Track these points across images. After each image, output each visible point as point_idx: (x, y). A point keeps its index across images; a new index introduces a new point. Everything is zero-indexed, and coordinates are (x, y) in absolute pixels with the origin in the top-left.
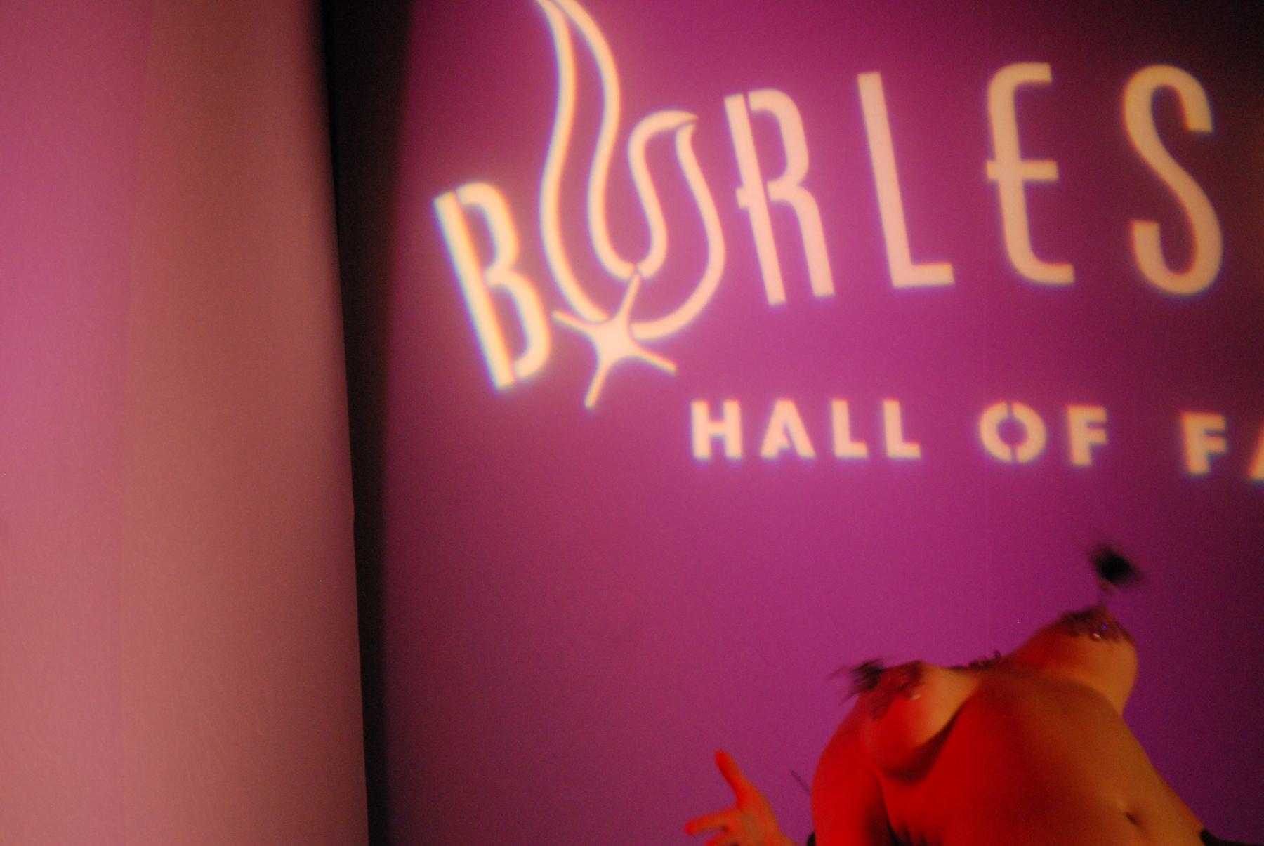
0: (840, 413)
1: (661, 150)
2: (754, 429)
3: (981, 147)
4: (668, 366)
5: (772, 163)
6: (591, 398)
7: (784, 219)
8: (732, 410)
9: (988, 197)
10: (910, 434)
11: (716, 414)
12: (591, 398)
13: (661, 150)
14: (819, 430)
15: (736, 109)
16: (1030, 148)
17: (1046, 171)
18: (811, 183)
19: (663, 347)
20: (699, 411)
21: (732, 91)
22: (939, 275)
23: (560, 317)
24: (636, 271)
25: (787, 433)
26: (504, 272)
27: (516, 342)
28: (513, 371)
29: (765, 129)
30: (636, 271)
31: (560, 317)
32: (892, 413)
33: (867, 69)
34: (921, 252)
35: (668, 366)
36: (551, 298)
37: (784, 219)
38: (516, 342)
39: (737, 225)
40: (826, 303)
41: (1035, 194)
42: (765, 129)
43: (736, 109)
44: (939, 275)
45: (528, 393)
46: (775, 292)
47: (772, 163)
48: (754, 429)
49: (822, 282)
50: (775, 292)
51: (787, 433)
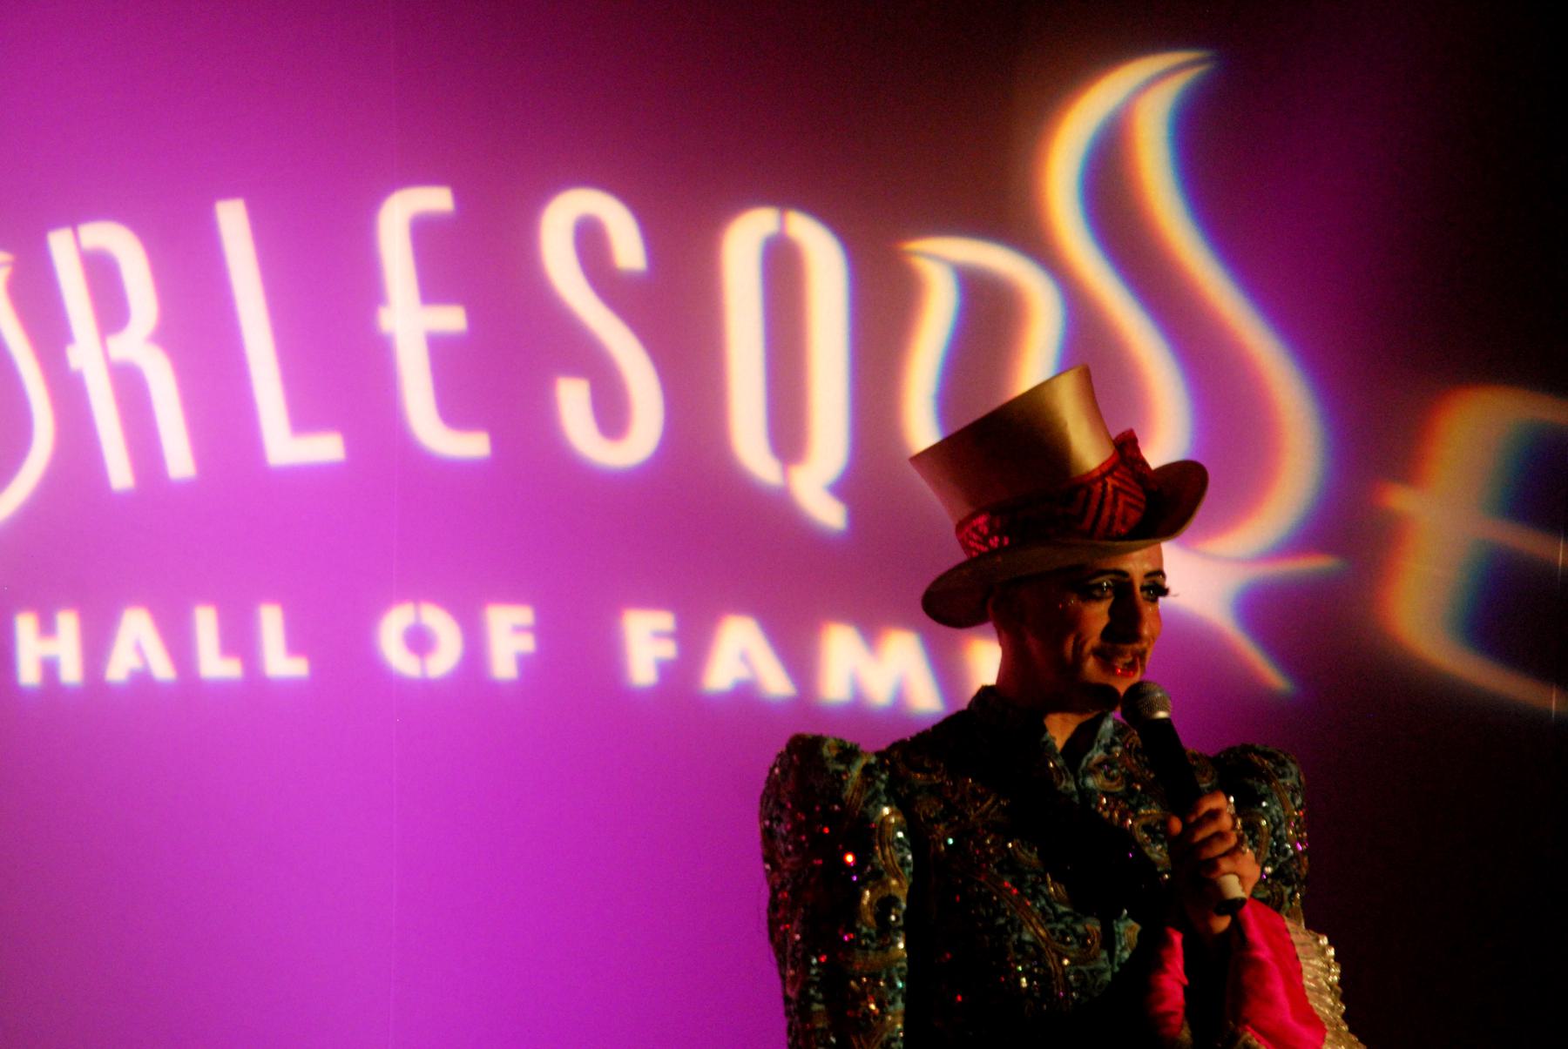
0: (206, 623)
2: (96, 646)
7: (129, 385)
8: (68, 623)
10: (296, 644)
11: (47, 628)
14: (180, 644)
15: (63, 247)
16: (433, 290)
17: (452, 319)
18: (164, 337)
20: (25, 626)
21: (57, 224)
22: (326, 448)
25: (139, 649)
29: (101, 271)
32: (271, 621)
34: (304, 420)
37: (129, 385)
40: (185, 487)
41: (439, 347)
42: (101, 271)
43: (63, 247)
44: (326, 448)
48: (96, 646)
49: (180, 461)
50: (120, 473)
51: (139, 649)
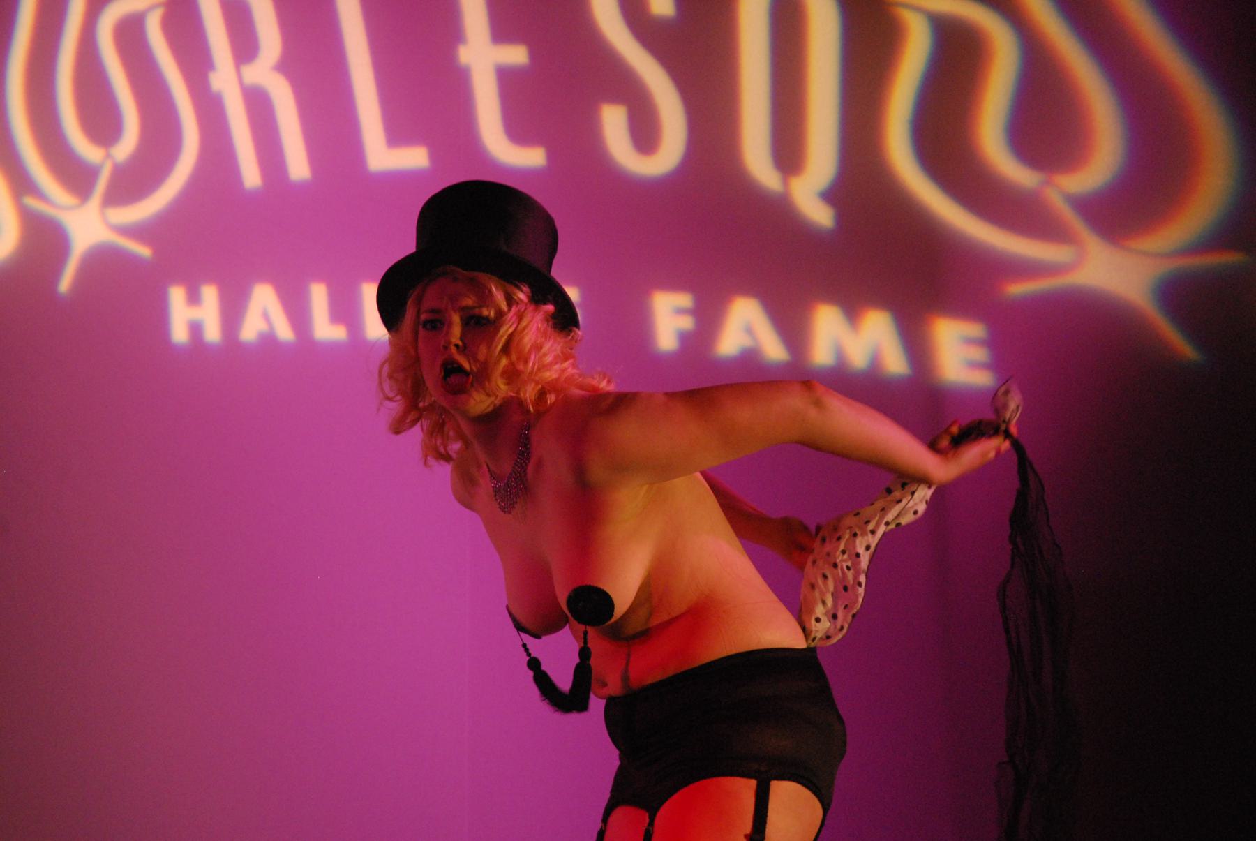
0: (319, 295)
2: (232, 313)
3: (452, 32)
4: (144, 251)
5: (245, 47)
6: (65, 284)
7: (258, 103)
8: (210, 294)
11: (194, 298)
12: (65, 284)
14: (298, 313)
16: (501, 33)
17: (516, 55)
18: (285, 66)
19: (137, 232)
20: (177, 296)
22: (415, 158)
23: (30, 202)
24: (108, 156)
25: (266, 317)
30: (108, 156)
31: (30, 202)
34: (397, 136)
35: (144, 251)
37: (258, 103)
40: (303, 187)
41: (506, 77)
44: (415, 158)
46: (251, 176)
47: (245, 47)
48: (232, 313)
49: (298, 166)
50: (251, 176)
51: (266, 317)
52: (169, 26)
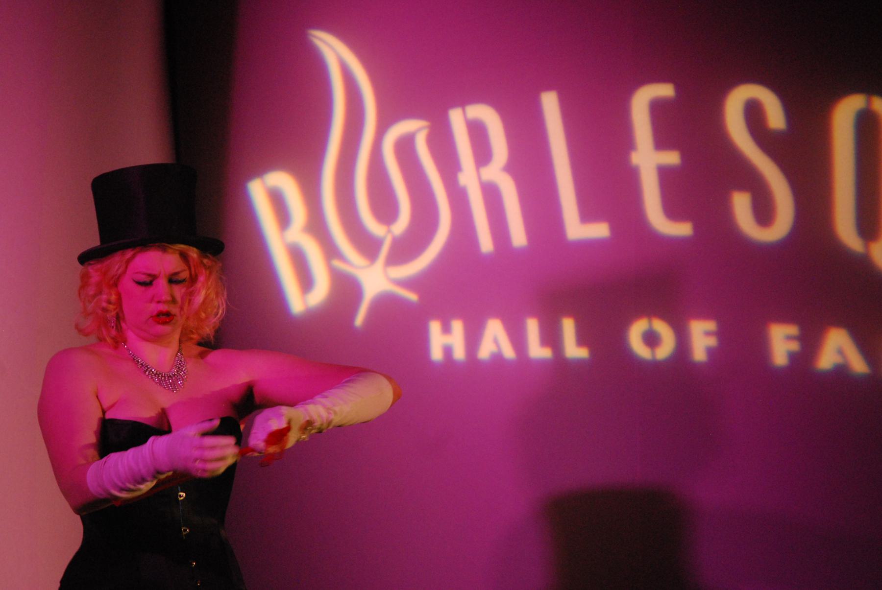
0: (532, 327)
1: (405, 147)
2: (473, 339)
3: (627, 142)
4: (412, 297)
5: (483, 155)
6: (359, 320)
7: (491, 194)
8: (457, 326)
9: (631, 177)
10: (582, 340)
11: (446, 329)
12: (359, 320)
13: (405, 147)
14: (518, 339)
15: (457, 118)
16: (661, 142)
17: (672, 158)
18: (510, 168)
19: (409, 284)
20: (435, 327)
21: (454, 105)
22: (600, 231)
23: (337, 264)
24: (389, 231)
25: (496, 341)
26: (297, 233)
27: (306, 281)
28: (304, 301)
29: (477, 131)
30: (389, 231)
31: (337, 264)
32: (568, 327)
33: (548, 88)
34: (587, 215)
35: (412, 297)
36: (331, 251)
37: (491, 194)
38: (306, 281)
39: (458, 198)
40: (521, 252)
41: (665, 174)
42: (477, 131)
43: (457, 118)
44: (600, 231)
45: (315, 317)
46: (486, 244)
47: (483, 155)
48: (473, 339)
49: (519, 237)
50: (486, 244)
51: (496, 341)
52: (432, 142)
